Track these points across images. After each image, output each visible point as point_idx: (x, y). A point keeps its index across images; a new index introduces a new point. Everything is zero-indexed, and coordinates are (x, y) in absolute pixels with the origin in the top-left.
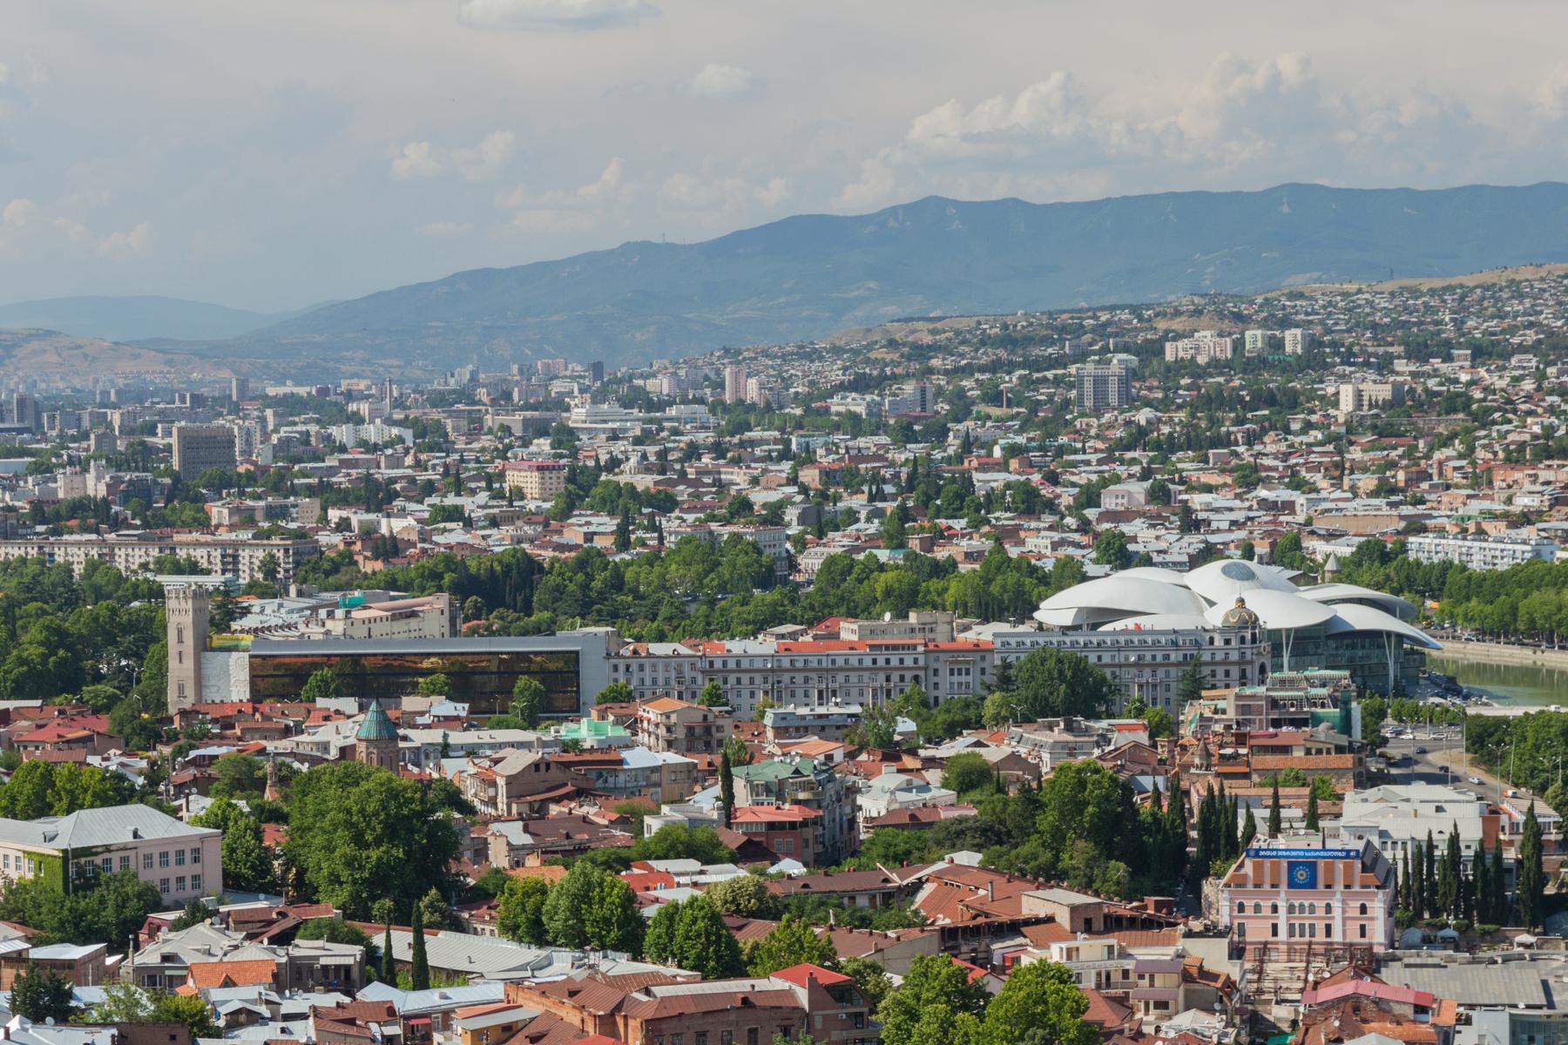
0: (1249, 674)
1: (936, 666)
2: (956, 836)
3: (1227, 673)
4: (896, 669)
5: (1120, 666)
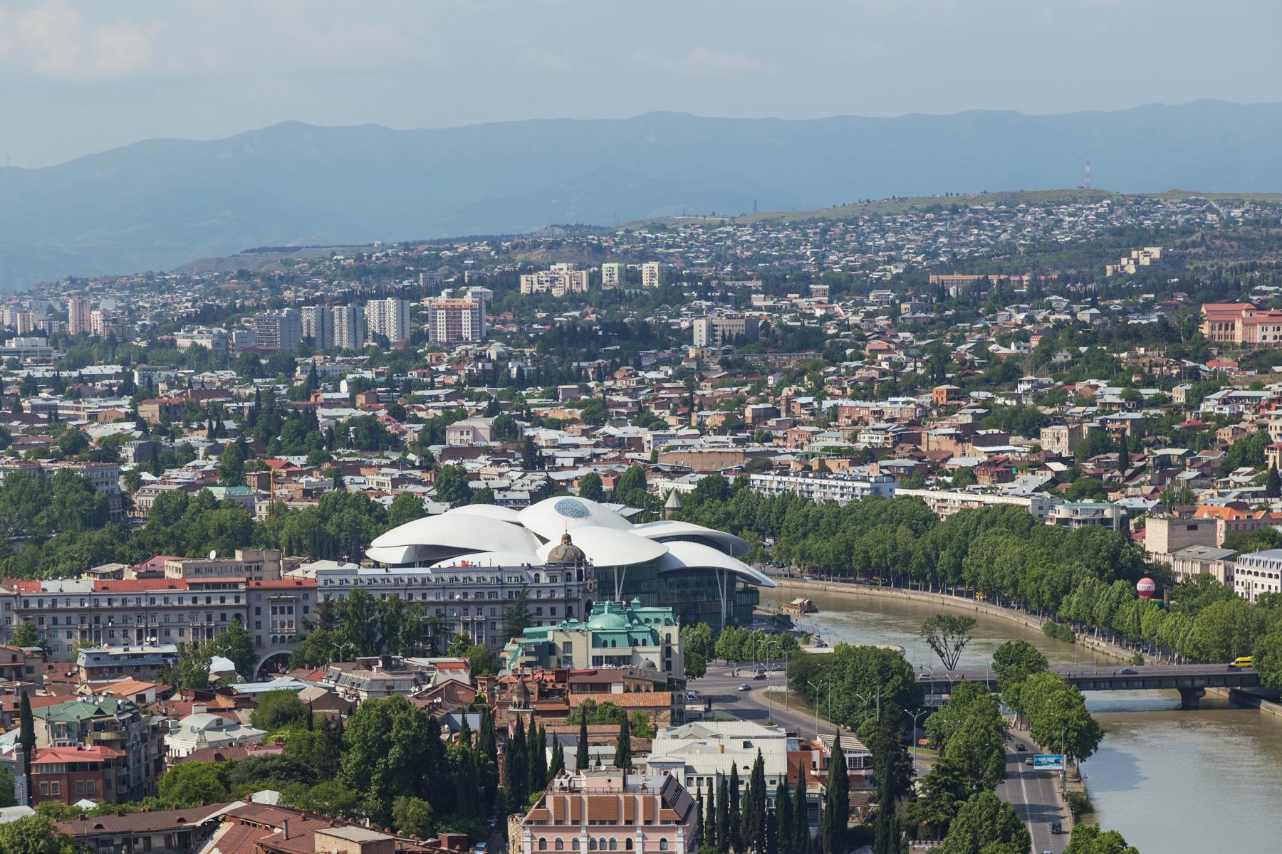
0: (575, 612)
1: (259, 604)
2: (261, 774)
3: (553, 611)
4: (216, 607)
5: (445, 604)
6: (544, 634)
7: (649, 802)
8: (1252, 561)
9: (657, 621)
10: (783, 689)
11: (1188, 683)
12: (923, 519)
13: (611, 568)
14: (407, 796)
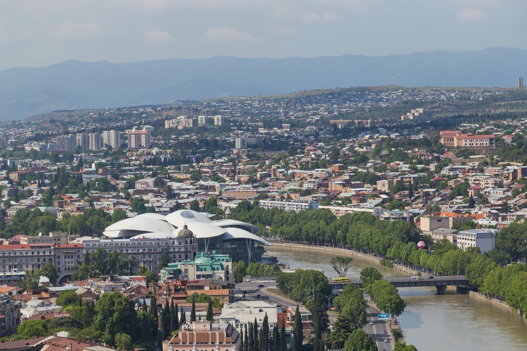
0: (189, 256)
1: (59, 254)
2: (60, 324)
3: (180, 256)
4: (42, 256)
5: (136, 254)
6: (177, 266)
7: (221, 335)
8: (464, 234)
9: (223, 260)
10: (275, 287)
11: (440, 284)
12: (330, 218)
13: (203, 238)
14: (121, 333)
